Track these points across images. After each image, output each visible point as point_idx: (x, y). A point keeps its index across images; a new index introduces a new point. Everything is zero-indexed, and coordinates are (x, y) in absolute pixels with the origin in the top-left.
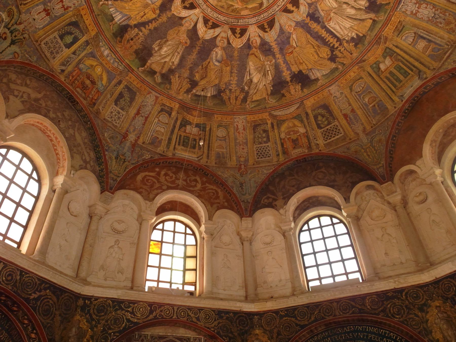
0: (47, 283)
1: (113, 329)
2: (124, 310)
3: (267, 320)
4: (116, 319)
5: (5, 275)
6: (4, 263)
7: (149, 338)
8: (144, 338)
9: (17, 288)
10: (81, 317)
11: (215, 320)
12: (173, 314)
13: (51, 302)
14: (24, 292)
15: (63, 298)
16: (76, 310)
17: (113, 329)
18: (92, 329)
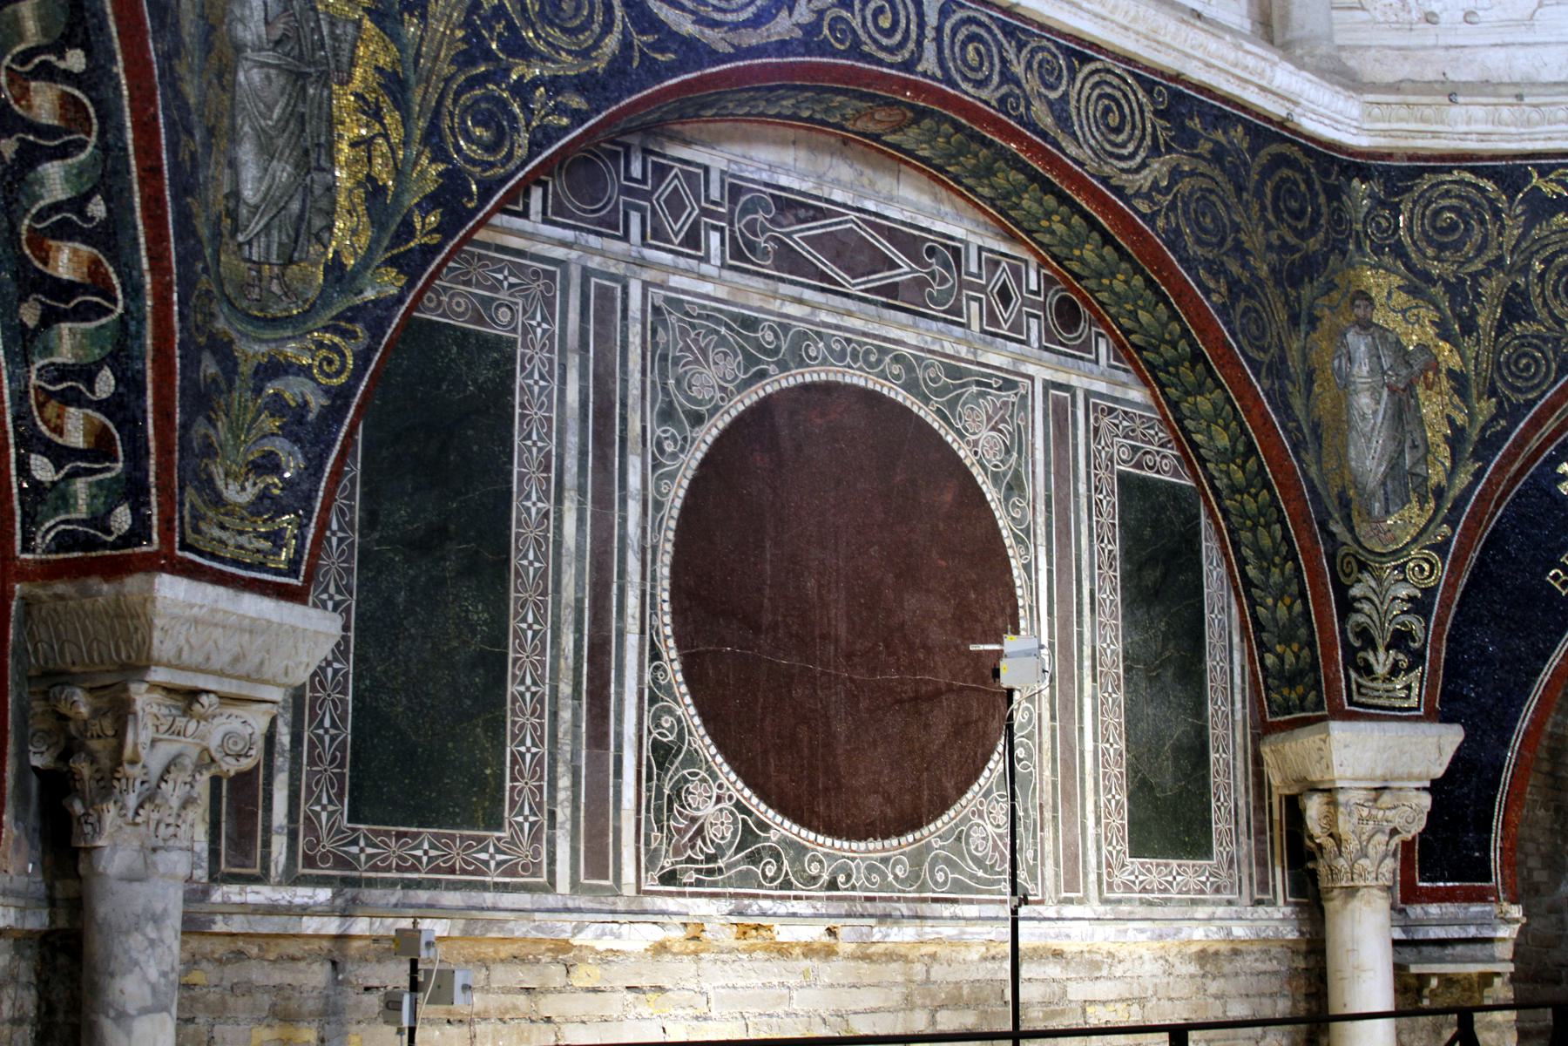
1: (544, 58)
3: (1437, 213)
8: (685, 191)
11: (1155, 151)
12: (919, 44)
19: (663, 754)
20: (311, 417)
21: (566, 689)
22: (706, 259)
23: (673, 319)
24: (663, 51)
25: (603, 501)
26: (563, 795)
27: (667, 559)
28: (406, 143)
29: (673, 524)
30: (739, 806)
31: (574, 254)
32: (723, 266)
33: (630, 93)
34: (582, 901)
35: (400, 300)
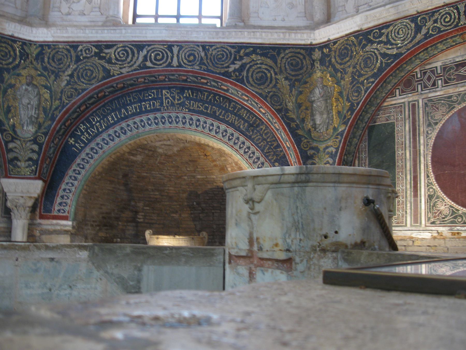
0: (247, 47)
1: (365, 75)
2: (375, 42)
4: (366, 60)
5: (185, 57)
6: (178, 46)
7: (439, 71)
9: (205, 65)
10: (322, 73)
12: (459, 18)
13: (264, 66)
14: (218, 67)
15: (283, 58)
16: (313, 65)
17: (365, 75)
18: (338, 83)
19: (430, 197)
20: (333, 153)
21: (408, 187)
22: (438, 87)
23: (429, 104)
24: (389, 60)
25: (415, 147)
26: (408, 208)
27: (430, 156)
28: (343, 103)
29: (431, 148)
30: (451, 206)
31: (406, 100)
32: (443, 87)
33: (383, 72)
34: (413, 228)
35: (345, 129)
